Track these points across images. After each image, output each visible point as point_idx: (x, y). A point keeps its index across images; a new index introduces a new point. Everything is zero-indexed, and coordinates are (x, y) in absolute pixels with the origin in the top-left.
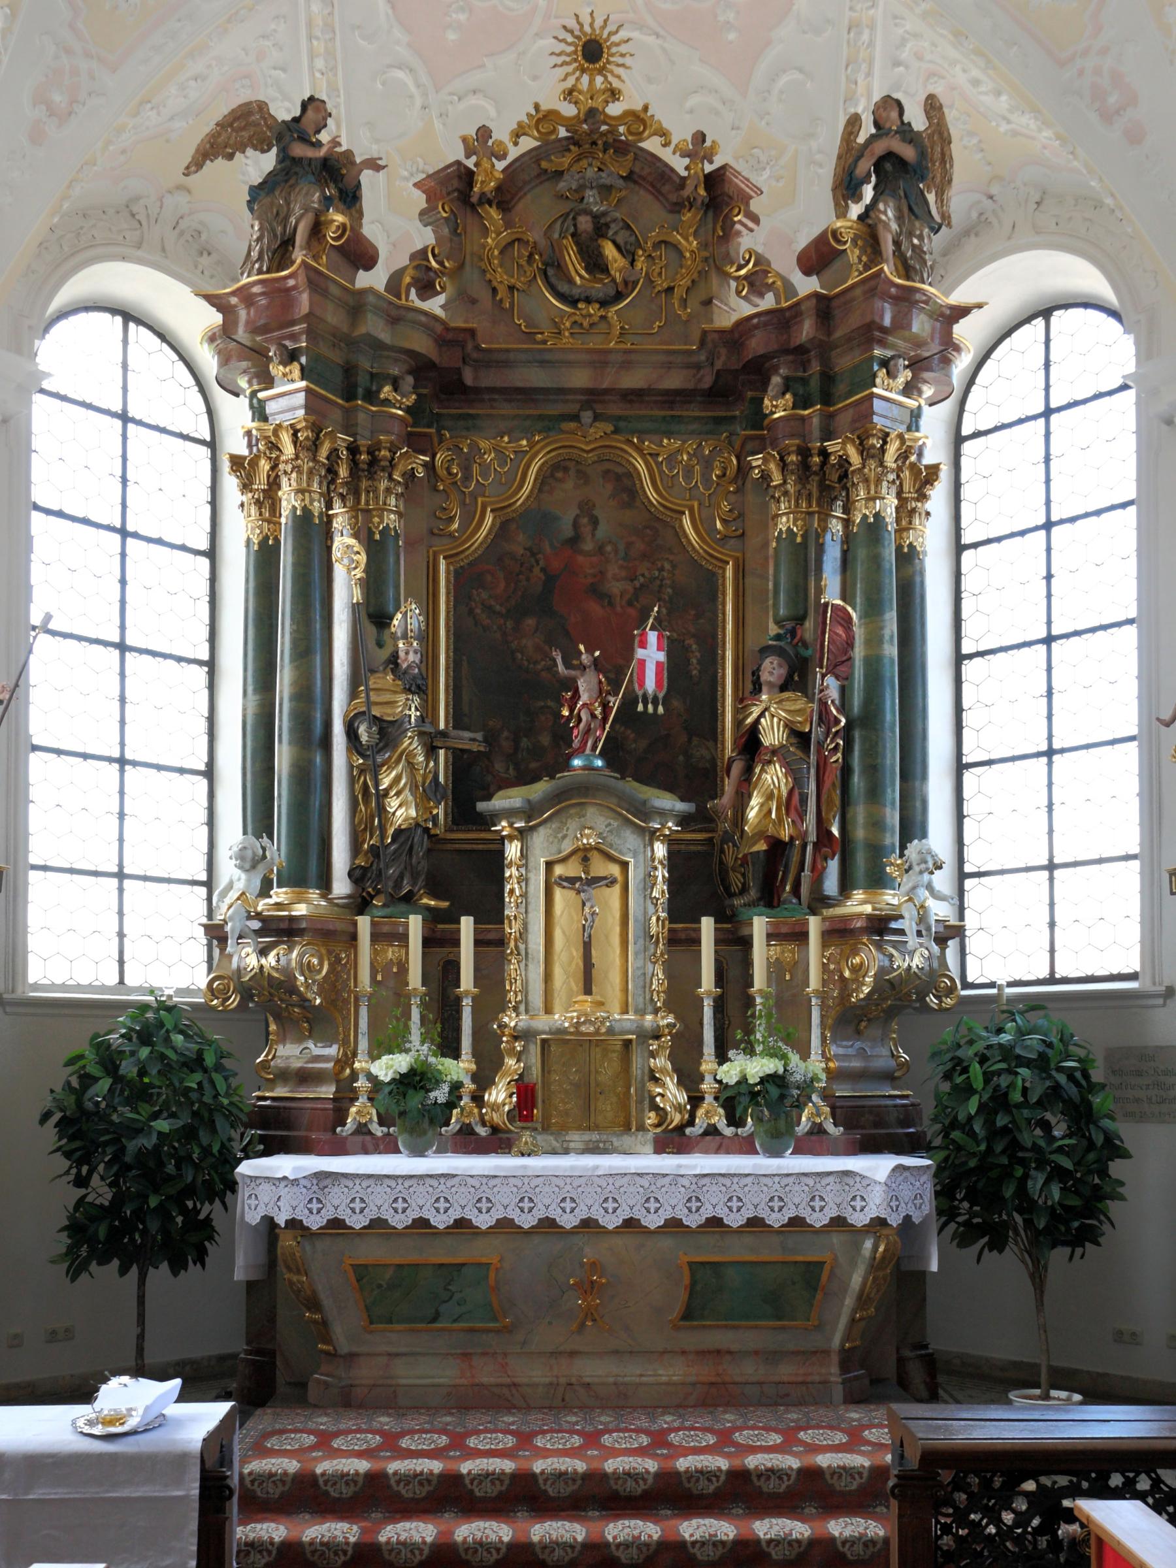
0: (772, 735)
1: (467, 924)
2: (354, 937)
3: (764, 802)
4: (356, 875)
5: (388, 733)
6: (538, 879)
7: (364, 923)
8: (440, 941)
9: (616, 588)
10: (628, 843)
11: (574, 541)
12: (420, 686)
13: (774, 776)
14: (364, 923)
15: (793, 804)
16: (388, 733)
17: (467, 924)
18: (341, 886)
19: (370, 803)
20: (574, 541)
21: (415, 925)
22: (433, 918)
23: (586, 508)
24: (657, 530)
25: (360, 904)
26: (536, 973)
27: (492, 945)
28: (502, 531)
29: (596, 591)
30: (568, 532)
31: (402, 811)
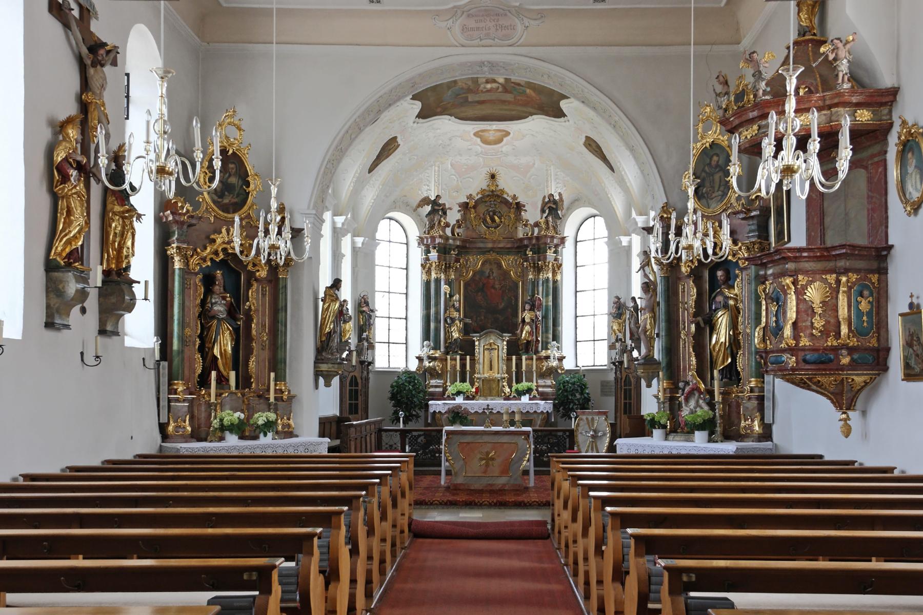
0: (527, 320)
1: (468, 357)
2: (446, 359)
3: (525, 333)
4: (446, 348)
5: (453, 320)
6: (482, 349)
7: (449, 357)
8: (463, 360)
9: (497, 286)
10: (499, 342)
11: (489, 276)
12: (458, 310)
13: (527, 328)
14: (449, 357)
15: (530, 333)
16: (453, 320)
17: (468, 357)
18: (442, 350)
19: (448, 333)
20: (489, 276)
21: (458, 357)
22: (461, 355)
23: (491, 270)
24: (506, 274)
25: (447, 353)
26: (481, 366)
27: (473, 360)
28: (474, 275)
29: (493, 287)
30: (487, 274)
31: (456, 335)
